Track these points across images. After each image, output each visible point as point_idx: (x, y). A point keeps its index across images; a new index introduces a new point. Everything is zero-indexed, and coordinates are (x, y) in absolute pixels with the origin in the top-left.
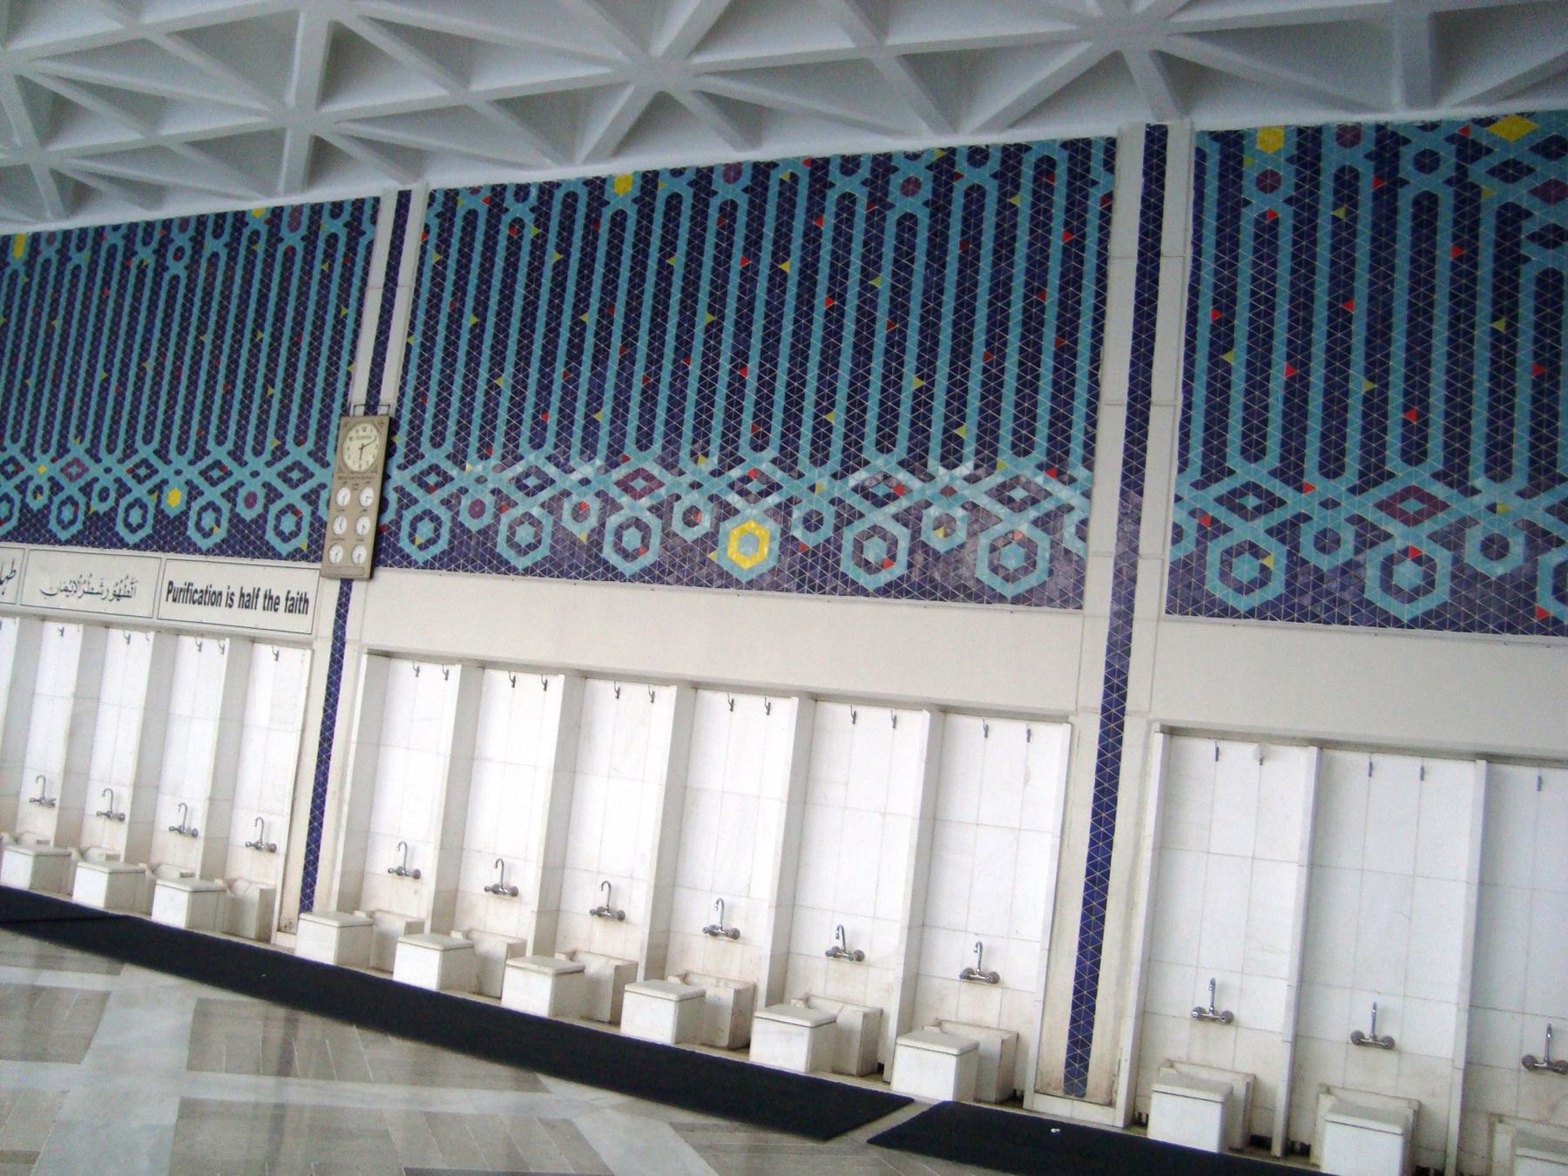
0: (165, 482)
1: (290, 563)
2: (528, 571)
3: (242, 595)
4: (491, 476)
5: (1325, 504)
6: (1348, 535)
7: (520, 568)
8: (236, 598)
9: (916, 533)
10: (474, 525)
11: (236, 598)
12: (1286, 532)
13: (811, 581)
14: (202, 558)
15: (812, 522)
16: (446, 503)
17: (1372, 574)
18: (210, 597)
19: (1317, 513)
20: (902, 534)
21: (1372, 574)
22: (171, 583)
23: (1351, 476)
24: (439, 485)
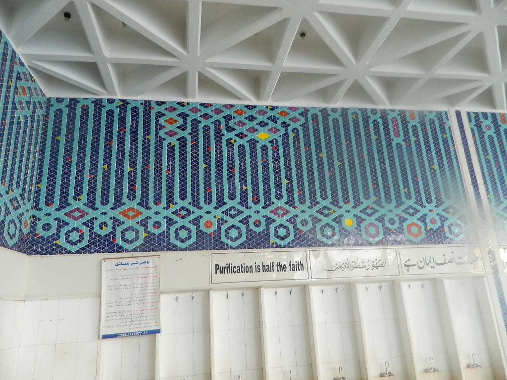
0: (341, 216)
1: (420, 246)
2: (79, 252)
3: (264, 266)
4: (213, 211)
5: (258, 212)
6: (164, 223)
7: (374, 243)
8: (261, 268)
9: (383, 225)
10: (305, 229)
11: (261, 268)
12: (245, 221)
13: (36, 250)
14: (234, 251)
15: (392, 221)
16: (335, 220)
17: (172, 235)
18: (249, 269)
19: (300, 215)
20: (193, 228)
21: (172, 235)
22: (217, 265)
23: (262, 204)
24: (237, 215)
